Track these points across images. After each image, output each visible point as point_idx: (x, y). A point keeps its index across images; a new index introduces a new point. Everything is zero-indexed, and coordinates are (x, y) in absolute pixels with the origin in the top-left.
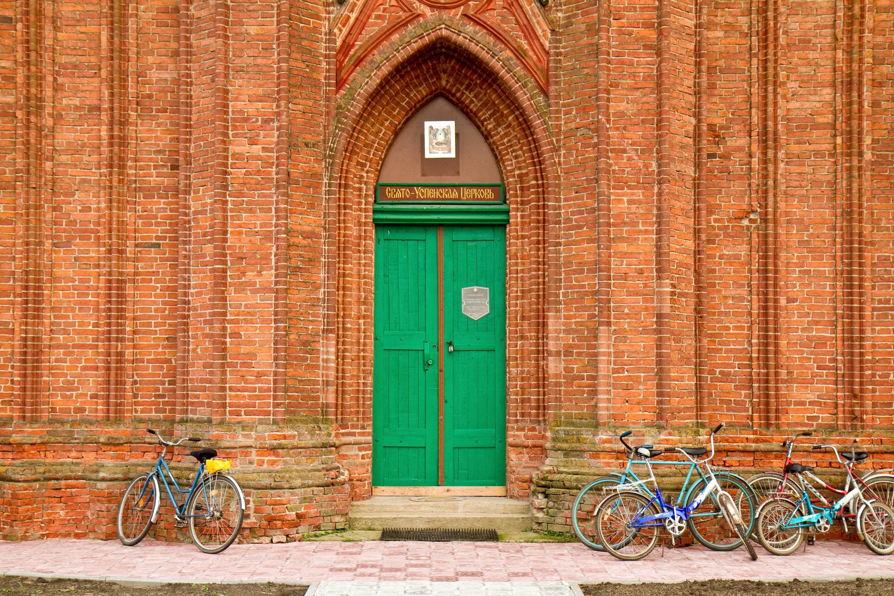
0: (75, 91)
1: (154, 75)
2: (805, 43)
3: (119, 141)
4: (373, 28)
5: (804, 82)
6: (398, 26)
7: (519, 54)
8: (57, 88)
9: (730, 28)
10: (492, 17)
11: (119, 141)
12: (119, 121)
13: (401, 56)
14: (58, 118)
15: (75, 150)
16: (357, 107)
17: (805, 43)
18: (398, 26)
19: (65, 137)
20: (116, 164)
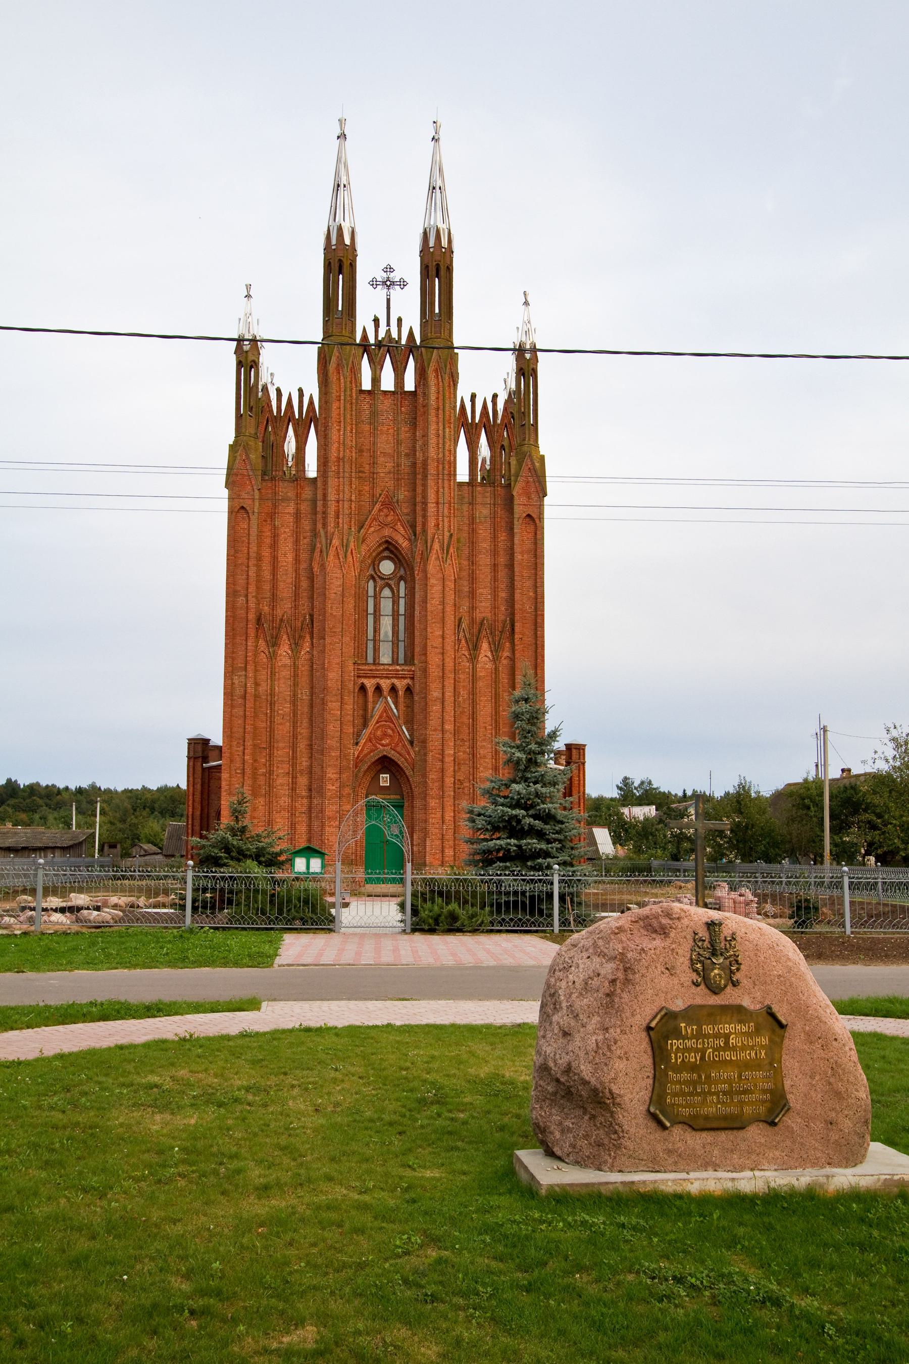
0: (282, 768)
1: (304, 764)
2: (485, 757)
3: (294, 783)
4: (365, 752)
5: (485, 768)
6: (372, 751)
7: (406, 759)
8: (278, 767)
9: (464, 752)
10: (398, 749)
11: (294, 783)
12: (294, 777)
13: (373, 760)
14: (277, 776)
15: (282, 785)
16: (361, 774)
17: (485, 757)
18: (372, 751)
19: (279, 781)
20: (293, 789)
